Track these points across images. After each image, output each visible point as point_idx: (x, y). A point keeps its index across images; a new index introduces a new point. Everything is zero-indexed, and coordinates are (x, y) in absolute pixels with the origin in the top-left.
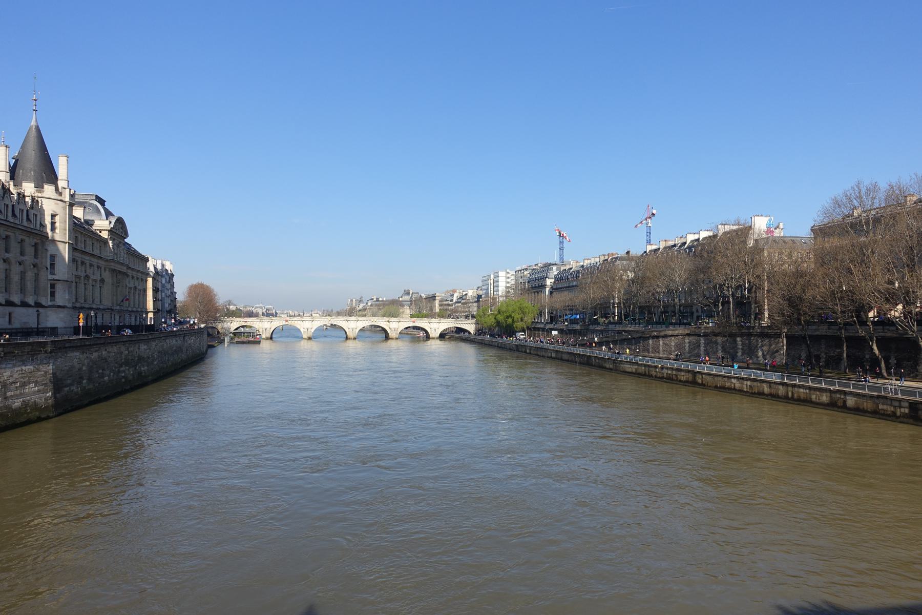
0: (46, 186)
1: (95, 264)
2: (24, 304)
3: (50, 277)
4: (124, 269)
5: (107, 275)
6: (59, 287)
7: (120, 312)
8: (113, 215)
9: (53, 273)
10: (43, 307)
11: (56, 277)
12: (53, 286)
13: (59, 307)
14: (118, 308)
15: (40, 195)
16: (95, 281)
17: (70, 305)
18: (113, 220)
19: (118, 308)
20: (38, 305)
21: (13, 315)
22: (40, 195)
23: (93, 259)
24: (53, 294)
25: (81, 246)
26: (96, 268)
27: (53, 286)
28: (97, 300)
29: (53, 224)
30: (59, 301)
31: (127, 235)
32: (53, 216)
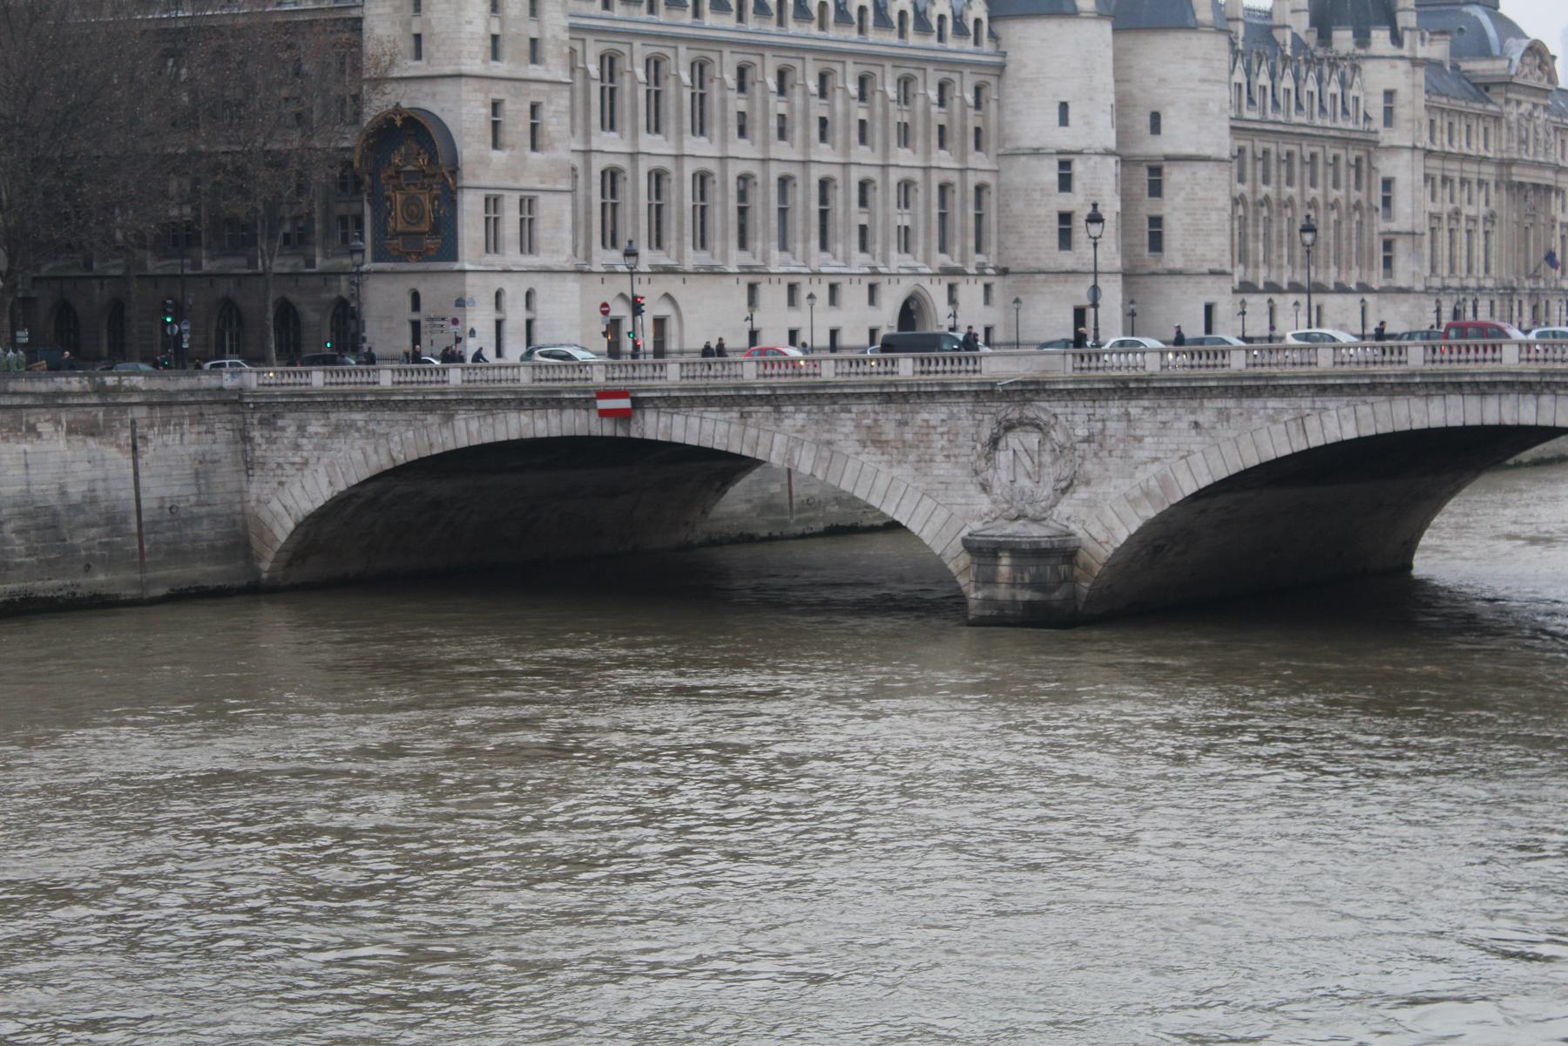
0: (1374, 33)
1: (1474, 177)
2: (1341, 289)
3: (1381, 225)
4: (1547, 177)
5: (1499, 200)
6: (1400, 246)
7: (1533, 293)
8: (1519, 33)
9: (1388, 216)
10: (1370, 291)
11: (1394, 227)
12: (1388, 245)
13: (1400, 290)
14: (1529, 284)
15: (1362, 52)
16: (1475, 220)
17: (1419, 286)
18: (1516, 49)
19: (1529, 284)
20: (1364, 288)
21: (1325, 310)
22: (1362, 52)
23: (1467, 167)
24: (1388, 262)
25: (1441, 143)
26: (1475, 186)
27: (1388, 245)
28: (1479, 266)
29: (1389, 113)
30: (1401, 279)
31: (1552, 78)
32: (1389, 95)
